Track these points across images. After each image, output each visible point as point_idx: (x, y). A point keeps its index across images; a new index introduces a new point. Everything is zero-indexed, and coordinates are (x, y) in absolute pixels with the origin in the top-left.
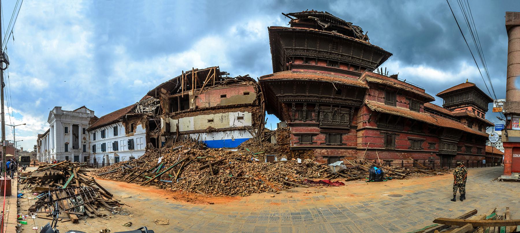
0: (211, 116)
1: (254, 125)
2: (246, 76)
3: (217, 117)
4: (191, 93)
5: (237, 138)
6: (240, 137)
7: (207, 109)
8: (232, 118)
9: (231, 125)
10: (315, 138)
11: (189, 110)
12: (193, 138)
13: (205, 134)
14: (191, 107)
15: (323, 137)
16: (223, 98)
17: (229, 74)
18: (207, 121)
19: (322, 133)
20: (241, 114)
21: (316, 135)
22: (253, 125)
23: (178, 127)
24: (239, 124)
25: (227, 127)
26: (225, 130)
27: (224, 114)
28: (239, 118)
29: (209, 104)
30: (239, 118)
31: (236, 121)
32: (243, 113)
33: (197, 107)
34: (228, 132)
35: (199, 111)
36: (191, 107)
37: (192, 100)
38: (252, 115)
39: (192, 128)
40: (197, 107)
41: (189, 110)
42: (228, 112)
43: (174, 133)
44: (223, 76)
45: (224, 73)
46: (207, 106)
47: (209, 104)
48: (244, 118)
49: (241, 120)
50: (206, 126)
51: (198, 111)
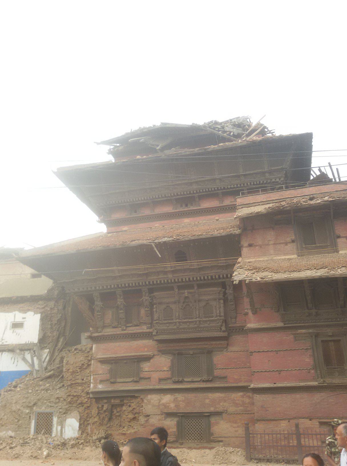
1: (42, 340)
10: (146, 366)
15: (164, 362)
19: (163, 352)
21: (148, 359)
28: (17, 325)
32: (24, 315)
38: (42, 319)
48: (26, 325)
49: (18, 330)
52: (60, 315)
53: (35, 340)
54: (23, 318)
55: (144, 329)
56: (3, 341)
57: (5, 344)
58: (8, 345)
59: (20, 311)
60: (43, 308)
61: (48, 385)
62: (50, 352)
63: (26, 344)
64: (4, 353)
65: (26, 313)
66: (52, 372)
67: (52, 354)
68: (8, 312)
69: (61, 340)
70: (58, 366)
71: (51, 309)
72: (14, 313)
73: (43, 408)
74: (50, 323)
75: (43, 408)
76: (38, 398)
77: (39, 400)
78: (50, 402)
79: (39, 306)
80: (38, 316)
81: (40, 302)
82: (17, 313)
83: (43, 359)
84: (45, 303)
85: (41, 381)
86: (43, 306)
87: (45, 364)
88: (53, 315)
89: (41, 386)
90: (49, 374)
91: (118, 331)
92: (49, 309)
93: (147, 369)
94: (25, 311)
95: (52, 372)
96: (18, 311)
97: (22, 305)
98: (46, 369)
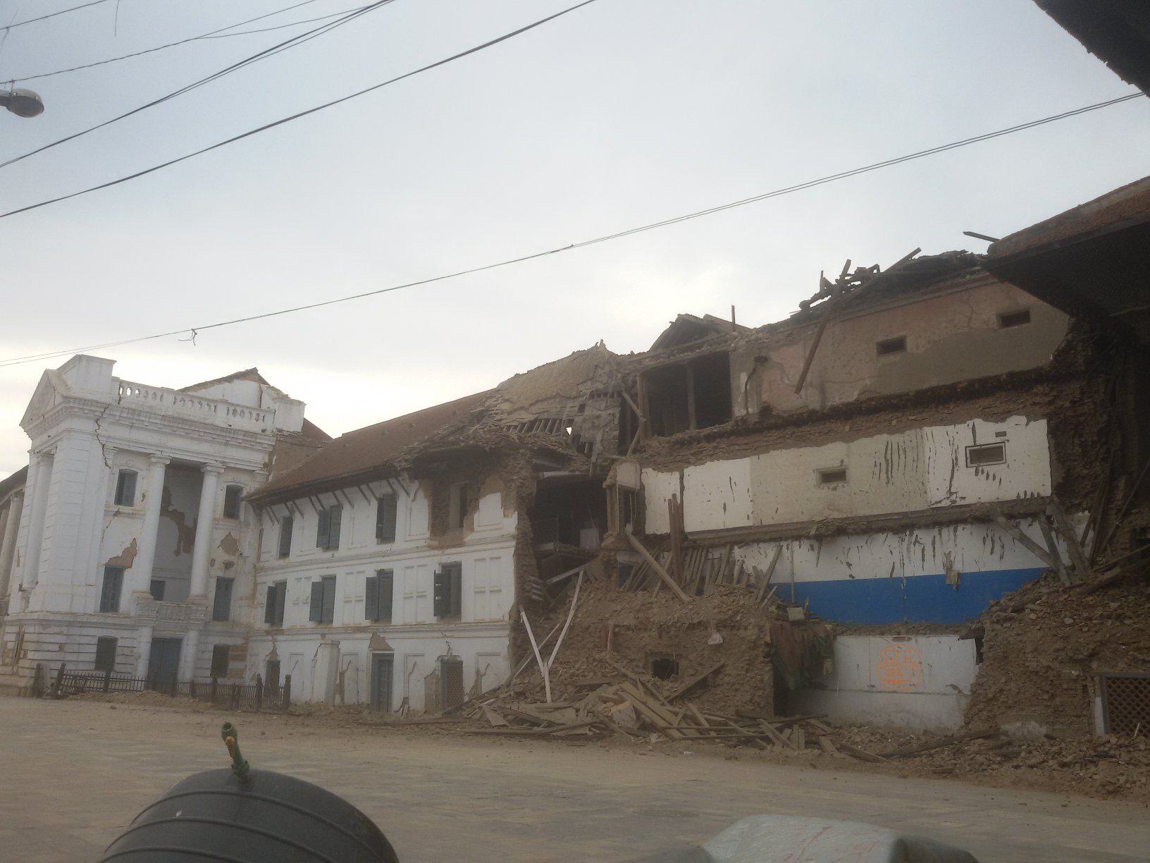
0: (831, 454)
1: (1062, 488)
3: (861, 454)
5: (970, 568)
6: (991, 564)
8: (938, 459)
9: (936, 493)
11: (728, 426)
12: (749, 567)
13: (806, 544)
18: (813, 478)
20: (986, 432)
23: (677, 511)
24: (976, 488)
25: (916, 505)
26: (902, 525)
27: (896, 439)
28: (983, 455)
29: (823, 391)
30: (983, 455)
32: (1000, 427)
33: (766, 410)
34: (925, 536)
35: (777, 427)
36: (739, 411)
37: (744, 377)
38: (1053, 433)
39: (739, 517)
40: (766, 410)
41: (728, 426)
43: (656, 542)
47: (823, 391)
48: (1009, 450)
49: (991, 468)
50: (812, 502)
52: (1105, 417)
54: (998, 435)
56: (953, 497)
57: (959, 502)
58: (969, 505)
60: (1050, 403)
61: (1114, 605)
62: (1092, 521)
63: (1018, 501)
64: (960, 528)
65: (1003, 420)
66: (1117, 571)
67: (1099, 524)
68: (954, 423)
69: (1122, 484)
70: (1128, 553)
71: (1073, 402)
72: (970, 423)
73: (1121, 665)
74: (1077, 441)
75: (1121, 665)
76: (1098, 637)
77: (1103, 643)
78: (1138, 649)
79: (1038, 399)
80: (1041, 426)
81: (1039, 389)
82: (978, 422)
83: (1079, 539)
84: (1052, 389)
85: (1090, 594)
86: (1047, 399)
87: (1087, 551)
88: (1082, 419)
89: (1093, 607)
90: (1109, 575)
92: (1067, 404)
94: (1001, 417)
95: (1117, 571)
96: (978, 417)
97: (986, 402)
98: (1093, 562)
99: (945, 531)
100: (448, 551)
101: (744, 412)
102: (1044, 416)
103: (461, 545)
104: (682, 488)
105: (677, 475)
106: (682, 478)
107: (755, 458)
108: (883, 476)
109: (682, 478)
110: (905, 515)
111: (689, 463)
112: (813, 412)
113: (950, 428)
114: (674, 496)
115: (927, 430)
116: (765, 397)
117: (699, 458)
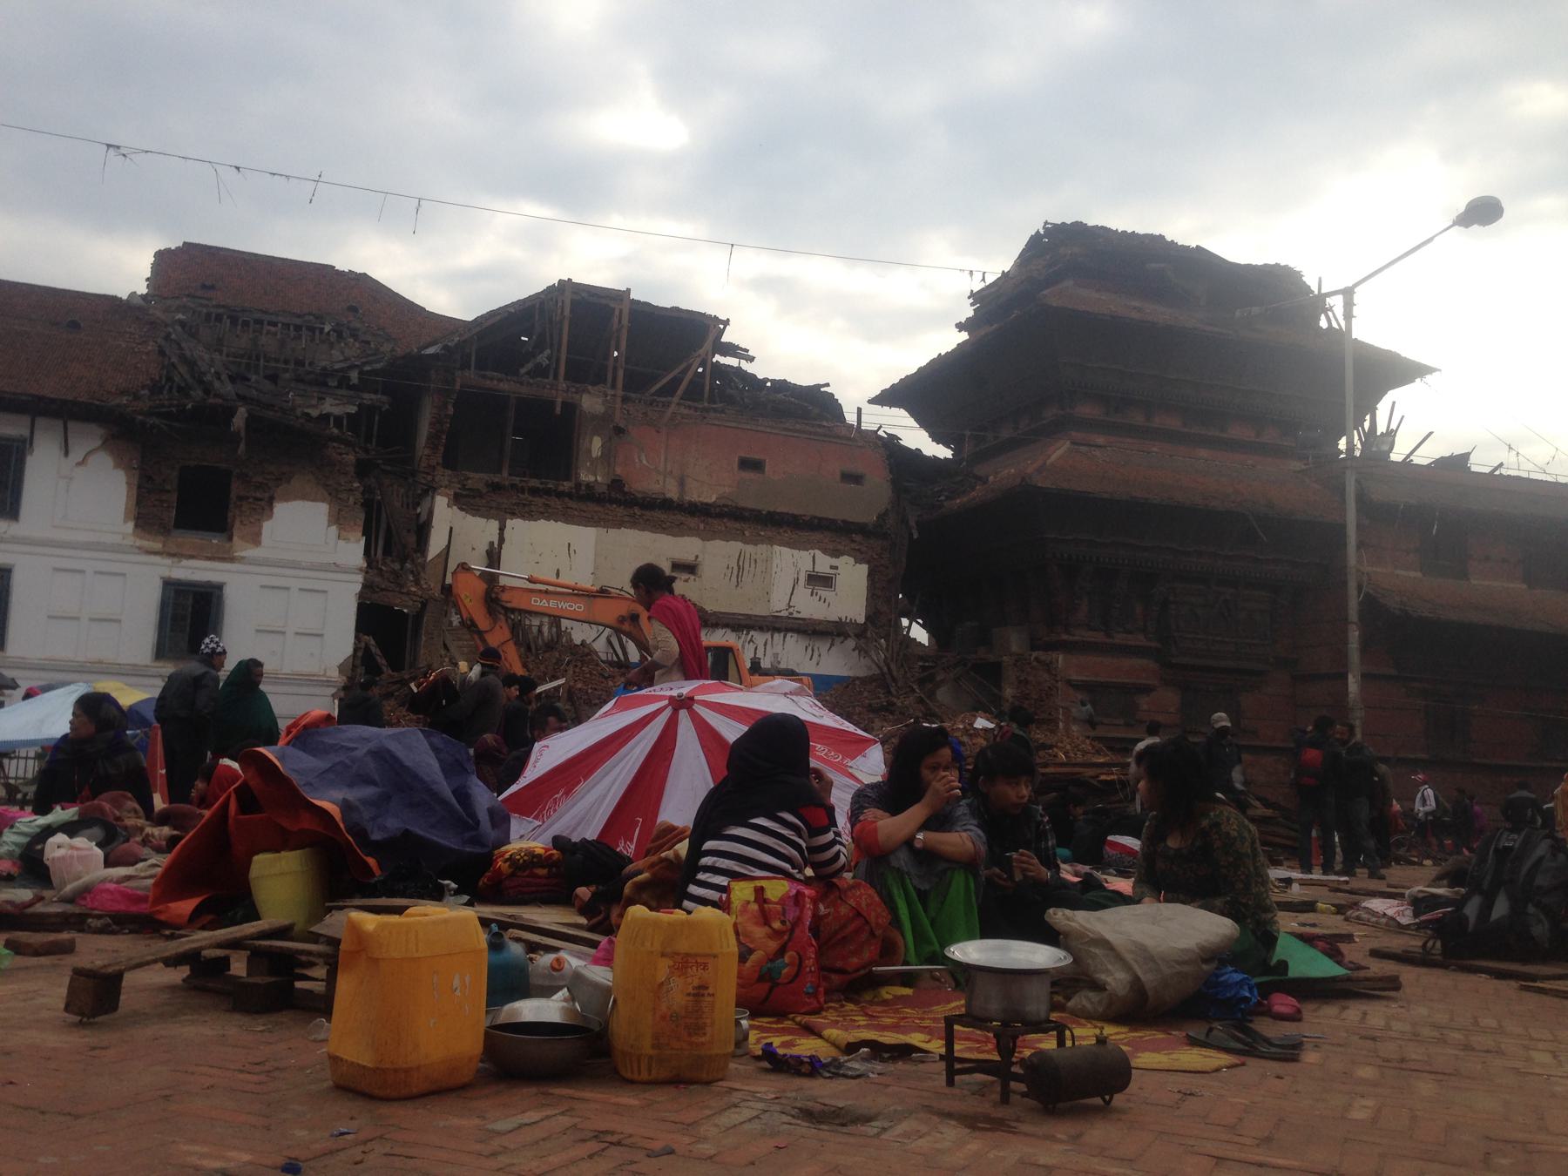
2: (819, 386)
4: (591, 403)
7: (666, 505)
9: (777, 604)
11: (566, 486)
14: (586, 477)
16: (749, 475)
17: (751, 359)
20: (824, 563)
21: (1147, 690)
22: (867, 618)
24: (809, 606)
25: (759, 610)
27: (749, 549)
28: (820, 581)
29: (682, 483)
30: (820, 581)
31: (803, 592)
32: (834, 562)
33: (617, 484)
35: (619, 503)
40: (617, 484)
41: (566, 486)
42: (771, 541)
44: (717, 358)
45: (731, 349)
46: (672, 493)
47: (682, 483)
49: (823, 593)
51: (618, 504)
53: (861, 620)
55: (1139, 640)
59: (825, 551)
82: (818, 552)
91: (1099, 637)
93: (1145, 707)
94: (836, 554)
99: (776, 635)
100: (185, 562)
101: (592, 478)
102: (868, 562)
103: (232, 560)
104: (502, 540)
105: (494, 525)
106: (502, 529)
107: (602, 531)
108: (734, 579)
109: (502, 529)
110: (749, 616)
111: (513, 515)
112: (671, 500)
113: (795, 552)
114: (492, 544)
115: (776, 548)
116: (619, 470)
117: (529, 514)
